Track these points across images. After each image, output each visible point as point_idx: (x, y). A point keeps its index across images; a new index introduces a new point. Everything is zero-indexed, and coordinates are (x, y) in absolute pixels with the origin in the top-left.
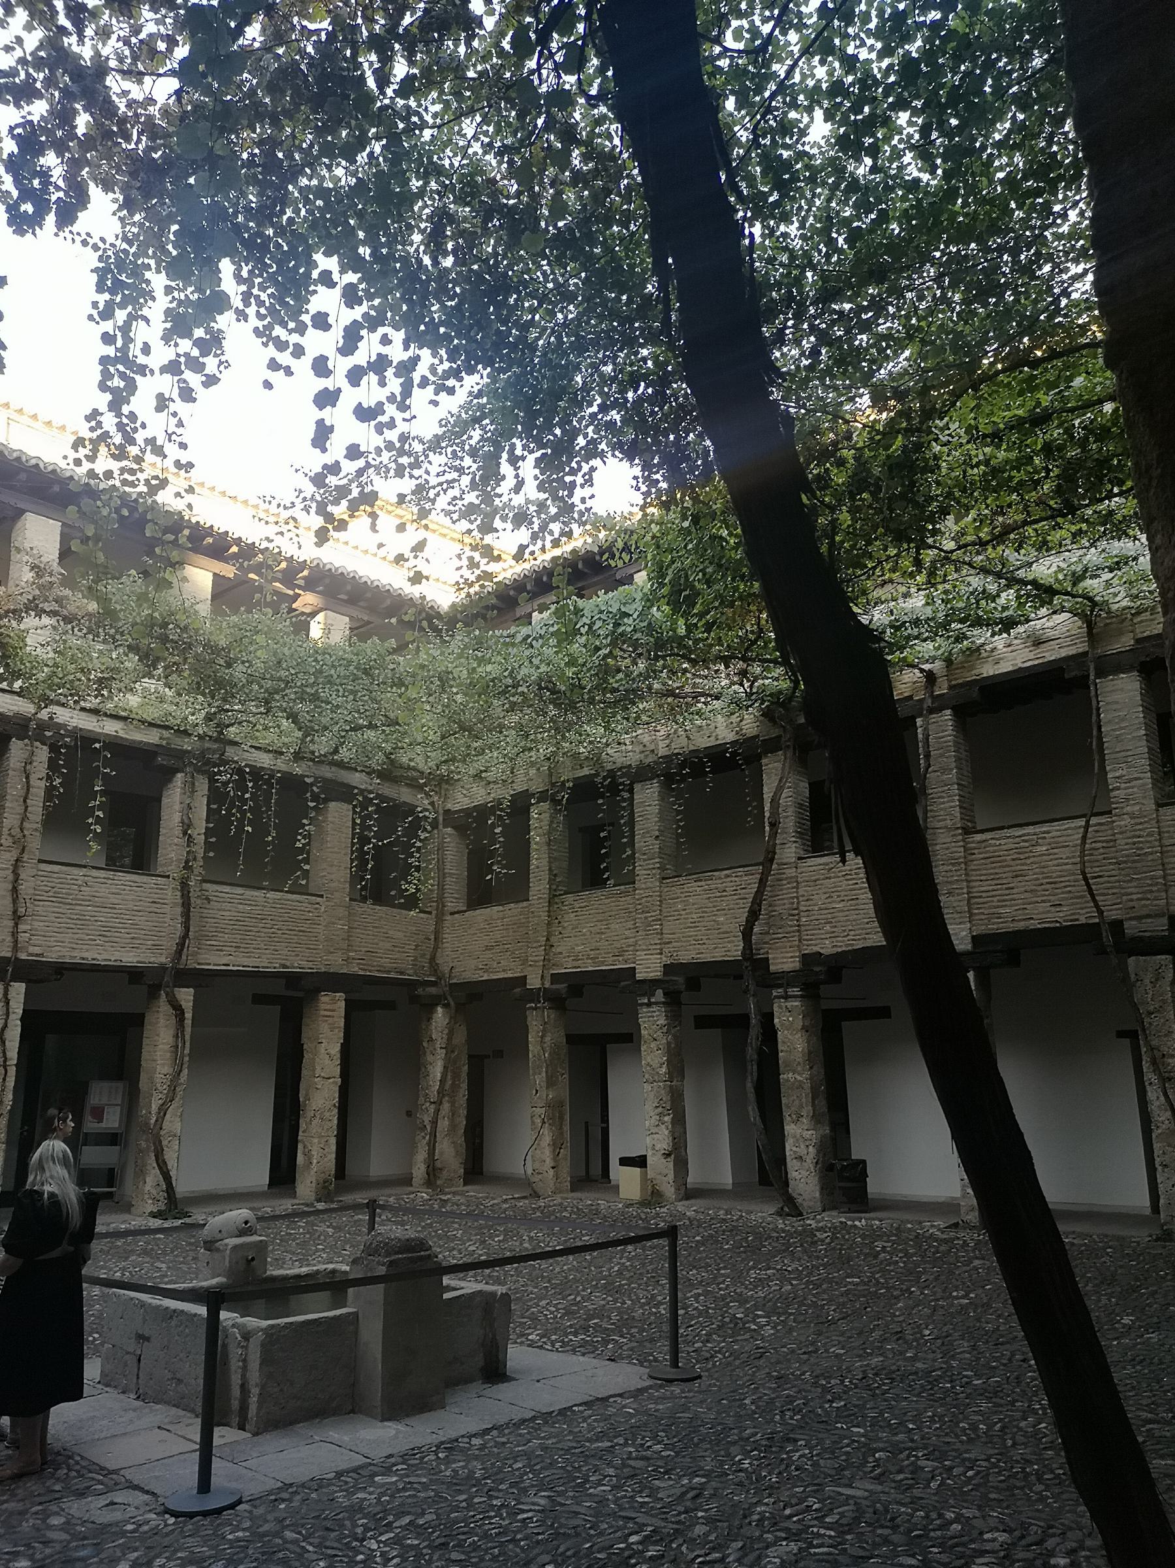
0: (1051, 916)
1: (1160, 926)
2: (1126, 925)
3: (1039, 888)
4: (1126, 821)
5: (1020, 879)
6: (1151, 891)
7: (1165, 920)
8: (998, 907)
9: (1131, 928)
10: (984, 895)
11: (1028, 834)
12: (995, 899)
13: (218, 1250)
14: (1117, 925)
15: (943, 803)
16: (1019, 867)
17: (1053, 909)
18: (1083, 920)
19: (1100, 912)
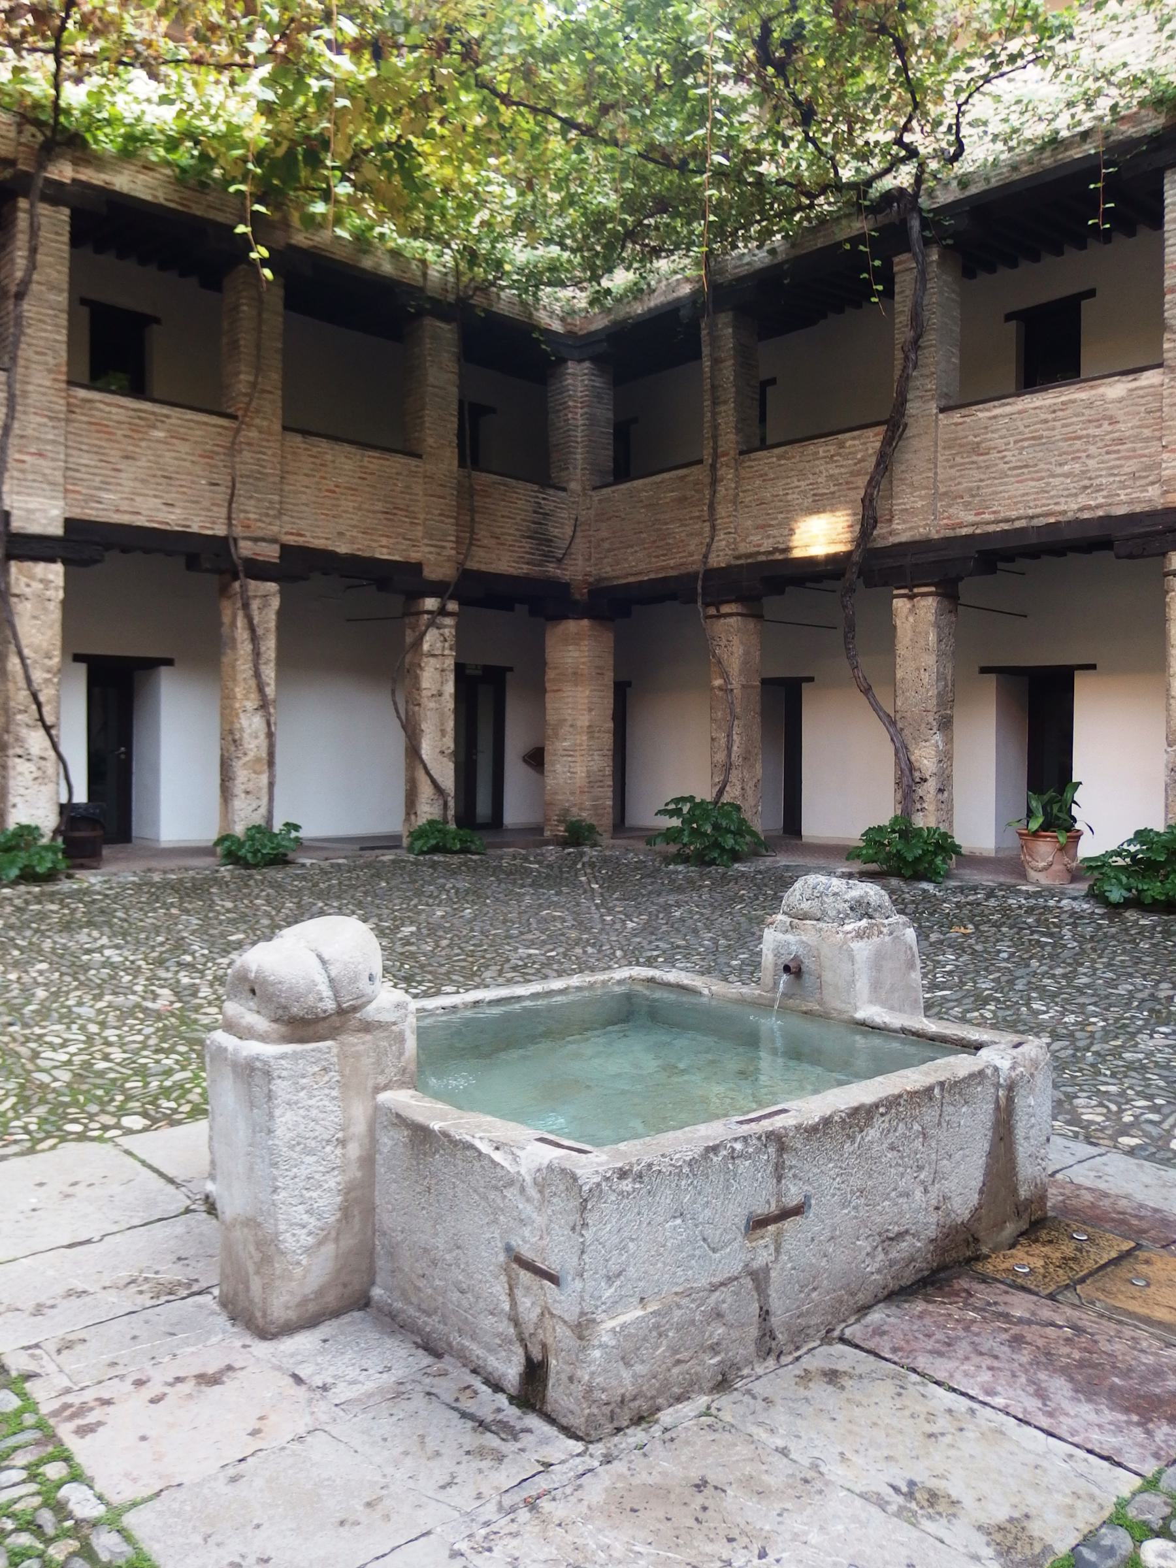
0: (161, 516)
1: (271, 553)
2: (242, 544)
3: (153, 480)
4: (253, 434)
5: (130, 462)
6: (267, 515)
7: (277, 547)
8: (100, 489)
9: (246, 549)
10: (83, 469)
11: (145, 411)
12: (98, 479)
13: (367, 1027)
14: (235, 540)
15: (45, 331)
16: (131, 448)
17: (164, 508)
18: (195, 528)
19: (230, 525)
